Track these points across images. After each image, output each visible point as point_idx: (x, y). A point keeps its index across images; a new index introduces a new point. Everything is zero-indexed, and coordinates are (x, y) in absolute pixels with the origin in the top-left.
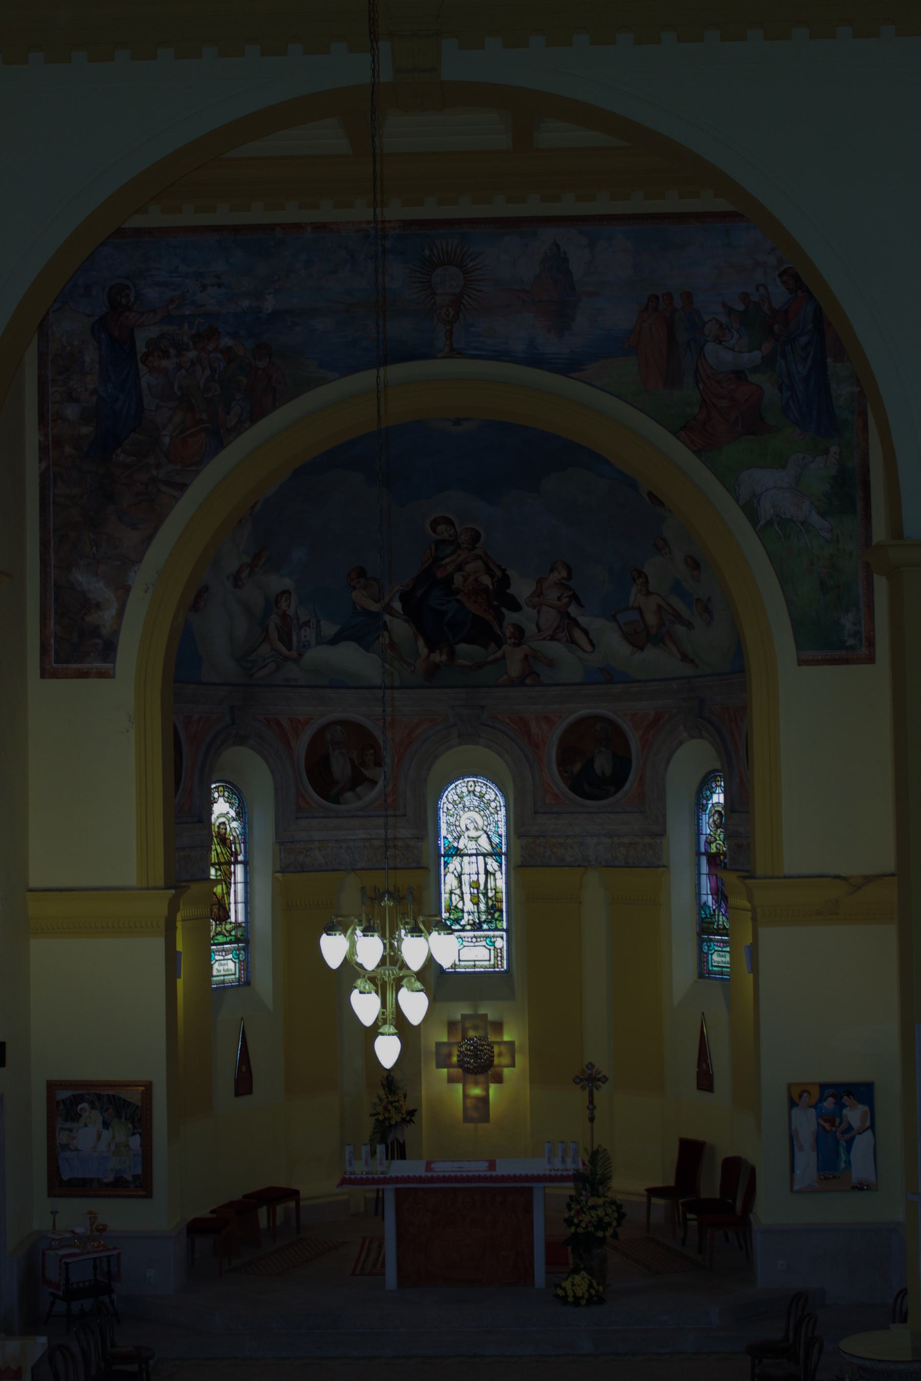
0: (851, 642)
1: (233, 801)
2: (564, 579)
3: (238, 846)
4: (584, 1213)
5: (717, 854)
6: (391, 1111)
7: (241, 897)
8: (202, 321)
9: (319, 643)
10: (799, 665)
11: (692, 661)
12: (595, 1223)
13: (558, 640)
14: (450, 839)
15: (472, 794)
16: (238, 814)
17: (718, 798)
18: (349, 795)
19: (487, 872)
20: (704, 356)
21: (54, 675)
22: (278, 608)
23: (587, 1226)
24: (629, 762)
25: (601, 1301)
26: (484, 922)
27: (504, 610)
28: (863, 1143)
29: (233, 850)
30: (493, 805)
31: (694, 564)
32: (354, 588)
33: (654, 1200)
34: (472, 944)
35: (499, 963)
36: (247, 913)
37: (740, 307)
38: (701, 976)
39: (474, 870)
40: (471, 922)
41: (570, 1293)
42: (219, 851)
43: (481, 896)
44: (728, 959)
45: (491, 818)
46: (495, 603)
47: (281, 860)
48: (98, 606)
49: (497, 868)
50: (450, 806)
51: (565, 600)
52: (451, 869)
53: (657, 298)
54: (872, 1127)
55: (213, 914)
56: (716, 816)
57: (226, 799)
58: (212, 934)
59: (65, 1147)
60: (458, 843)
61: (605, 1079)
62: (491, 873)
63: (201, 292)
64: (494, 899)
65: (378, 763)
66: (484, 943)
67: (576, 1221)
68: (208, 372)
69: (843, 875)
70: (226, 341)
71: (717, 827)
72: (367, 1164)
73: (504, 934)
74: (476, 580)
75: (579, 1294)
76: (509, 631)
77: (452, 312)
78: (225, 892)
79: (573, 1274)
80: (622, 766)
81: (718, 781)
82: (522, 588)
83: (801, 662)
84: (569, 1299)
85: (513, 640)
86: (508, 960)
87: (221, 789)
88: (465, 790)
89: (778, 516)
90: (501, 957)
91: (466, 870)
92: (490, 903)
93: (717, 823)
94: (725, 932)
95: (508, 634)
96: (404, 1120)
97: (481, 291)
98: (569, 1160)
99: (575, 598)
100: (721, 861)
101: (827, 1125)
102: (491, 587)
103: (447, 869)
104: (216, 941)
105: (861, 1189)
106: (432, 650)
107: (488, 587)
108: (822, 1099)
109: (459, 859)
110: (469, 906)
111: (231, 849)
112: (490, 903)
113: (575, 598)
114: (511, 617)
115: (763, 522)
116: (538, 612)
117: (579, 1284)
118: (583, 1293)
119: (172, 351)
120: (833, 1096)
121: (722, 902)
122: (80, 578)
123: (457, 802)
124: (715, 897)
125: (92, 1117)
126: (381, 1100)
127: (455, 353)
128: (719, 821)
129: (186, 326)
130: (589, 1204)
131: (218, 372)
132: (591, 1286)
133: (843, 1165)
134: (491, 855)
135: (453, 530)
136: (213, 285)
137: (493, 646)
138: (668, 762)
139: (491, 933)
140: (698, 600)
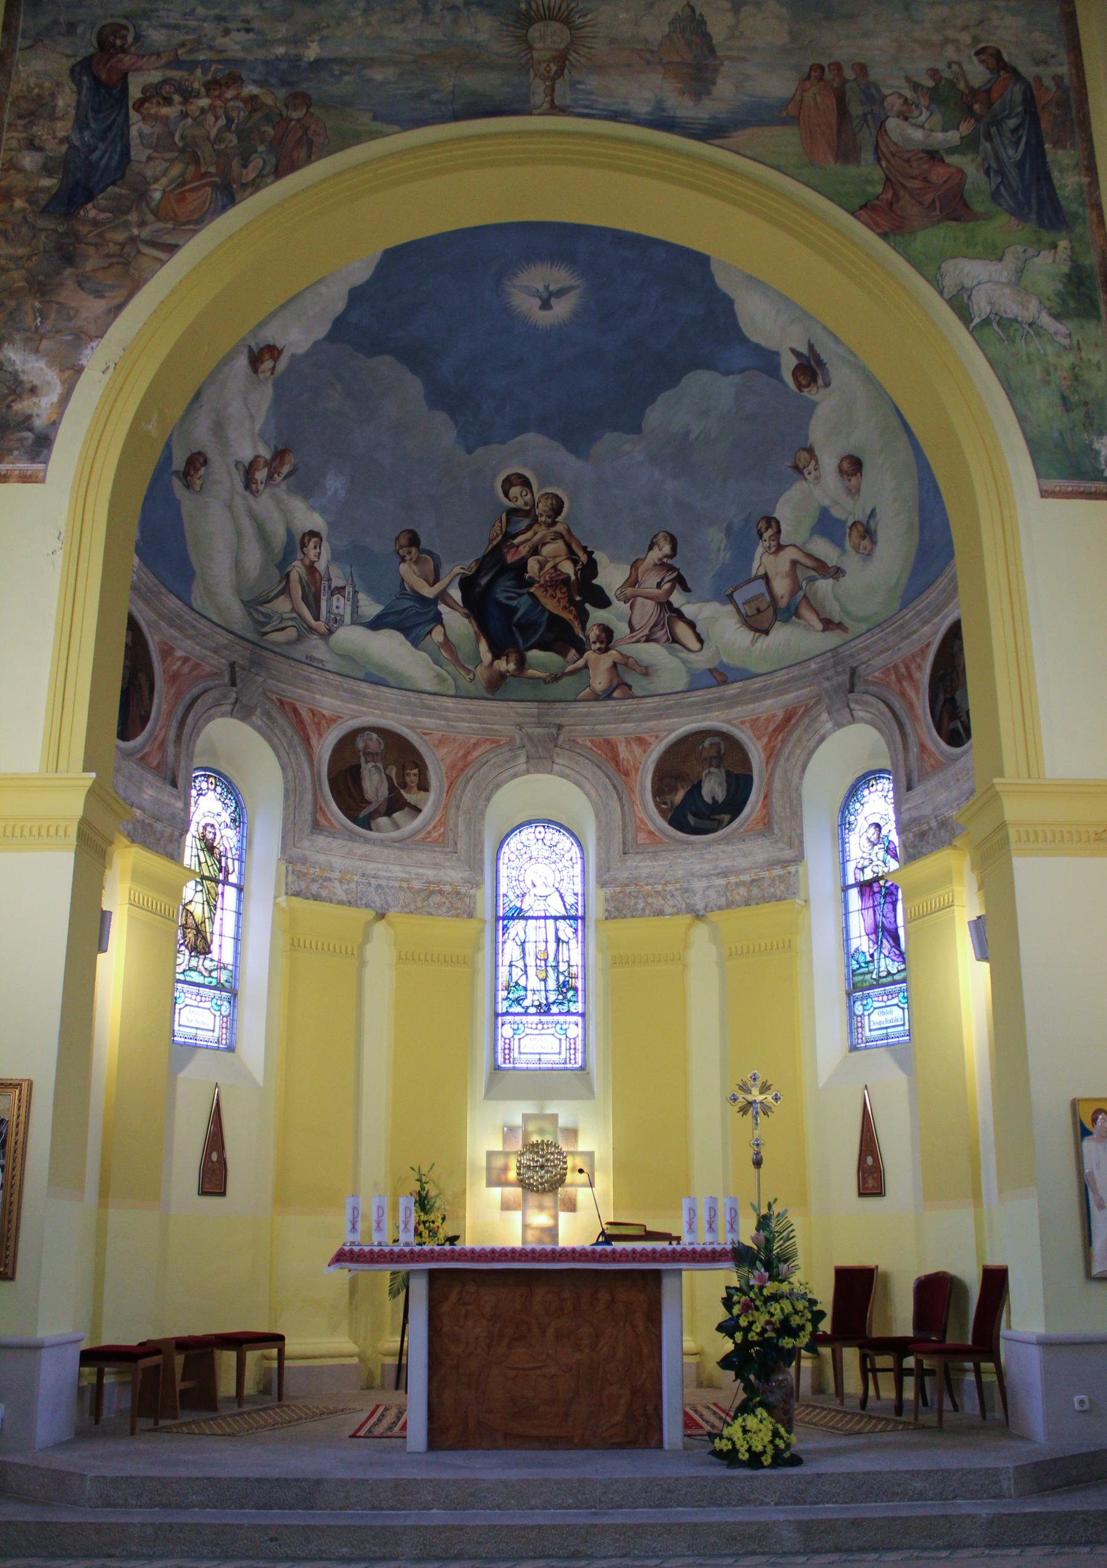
1: (226, 801)
2: (667, 556)
3: (230, 862)
4: (757, 1309)
5: (876, 879)
6: (423, 1234)
7: (229, 929)
8: (220, 67)
9: (354, 622)
10: (1042, 496)
11: (840, 625)
12: (778, 1325)
13: (656, 641)
14: (512, 897)
15: (540, 841)
16: (234, 820)
18: (383, 821)
19: (558, 940)
20: (886, 131)
22: (305, 554)
23: (764, 1330)
24: (748, 781)
25: (795, 1461)
26: (554, 1003)
27: (588, 606)
29: (223, 864)
30: (568, 856)
32: (403, 560)
34: (537, 1032)
35: (572, 1057)
36: (236, 954)
39: (542, 937)
40: (536, 1003)
41: (742, 1447)
42: (203, 859)
43: (549, 969)
45: (565, 873)
46: (578, 598)
47: (287, 884)
49: (571, 935)
50: (512, 857)
51: (667, 586)
52: (511, 937)
53: (822, 68)
55: (187, 939)
56: (872, 830)
57: (218, 797)
58: (180, 969)
60: (522, 901)
62: (563, 942)
63: (224, 36)
64: (566, 974)
65: (424, 787)
66: (552, 1031)
67: (743, 1322)
68: (222, 122)
70: (251, 89)
71: (874, 845)
73: (579, 1019)
74: (555, 567)
76: (593, 633)
77: (554, 68)
78: (207, 915)
79: (742, 1414)
81: (872, 786)
84: (740, 1456)
85: (598, 645)
86: (584, 1052)
87: (211, 780)
88: (532, 836)
89: (996, 314)
90: (575, 1049)
91: (531, 937)
92: (562, 978)
93: (872, 839)
94: (889, 979)
95: (592, 637)
97: (592, 48)
99: (680, 582)
100: (881, 887)
102: (573, 577)
103: (506, 935)
104: (188, 979)
106: (496, 656)
109: (522, 922)
110: (534, 983)
111: (220, 863)
112: (562, 978)
113: (680, 582)
114: (597, 615)
115: (976, 321)
116: (632, 607)
118: (765, 1447)
119: (177, 98)
121: (884, 941)
123: (522, 852)
124: (873, 937)
127: (555, 109)
128: (875, 836)
129: (199, 72)
130: (765, 1292)
131: (236, 121)
132: (776, 1434)
134: (564, 918)
135: (529, 496)
136: (239, 30)
138: (804, 768)
139: (562, 1019)
140: (854, 524)
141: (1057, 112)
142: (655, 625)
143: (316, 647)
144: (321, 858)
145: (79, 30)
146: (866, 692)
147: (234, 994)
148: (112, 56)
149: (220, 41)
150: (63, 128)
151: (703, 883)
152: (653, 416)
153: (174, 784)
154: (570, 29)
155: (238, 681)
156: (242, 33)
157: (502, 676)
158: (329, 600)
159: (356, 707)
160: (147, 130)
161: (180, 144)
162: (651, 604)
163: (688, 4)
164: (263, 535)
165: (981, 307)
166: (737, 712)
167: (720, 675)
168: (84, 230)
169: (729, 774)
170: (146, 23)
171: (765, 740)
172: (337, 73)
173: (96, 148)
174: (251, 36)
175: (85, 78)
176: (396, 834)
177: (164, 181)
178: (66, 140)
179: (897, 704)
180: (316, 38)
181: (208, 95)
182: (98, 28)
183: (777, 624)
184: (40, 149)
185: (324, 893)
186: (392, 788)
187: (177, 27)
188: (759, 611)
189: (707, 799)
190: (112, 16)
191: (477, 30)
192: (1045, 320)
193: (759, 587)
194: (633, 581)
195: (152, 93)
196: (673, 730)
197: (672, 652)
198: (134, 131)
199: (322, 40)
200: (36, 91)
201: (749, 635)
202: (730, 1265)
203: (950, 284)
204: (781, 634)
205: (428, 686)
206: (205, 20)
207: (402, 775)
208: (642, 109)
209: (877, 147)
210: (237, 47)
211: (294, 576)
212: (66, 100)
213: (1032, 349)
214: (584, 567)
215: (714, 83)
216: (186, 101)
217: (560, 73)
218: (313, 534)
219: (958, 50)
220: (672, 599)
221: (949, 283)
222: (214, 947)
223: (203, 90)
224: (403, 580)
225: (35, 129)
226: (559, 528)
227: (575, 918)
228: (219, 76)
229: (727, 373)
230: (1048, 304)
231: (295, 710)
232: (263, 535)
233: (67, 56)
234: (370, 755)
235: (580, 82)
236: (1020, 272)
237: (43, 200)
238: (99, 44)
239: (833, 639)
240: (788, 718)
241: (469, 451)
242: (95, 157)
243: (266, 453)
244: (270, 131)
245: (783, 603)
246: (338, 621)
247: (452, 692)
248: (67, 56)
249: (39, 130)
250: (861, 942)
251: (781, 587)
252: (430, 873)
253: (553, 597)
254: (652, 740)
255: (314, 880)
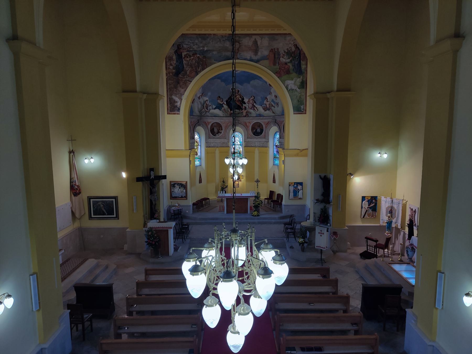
0: (302, 110)
5: (277, 145)
17: (278, 136)
18: (217, 135)
19: (239, 148)
21: (170, 114)
25: (259, 216)
28: (301, 192)
31: (276, 97)
32: (218, 100)
33: (266, 200)
37: (287, 51)
38: (274, 165)
44: (279, 162)
48: (177, 102)
53: (272, 49)
54: (302, 189)
59: (173, 192)
61: (255, 181)
65: (222, 130)
69: (300, 149)
70: (198, 55)
72: (222, 194)
75: (256, 215)
76: (244, 108)
80: (262, 131)
82: (246, 100)
83: (294, 114)
96: (226, 187)
98: (254, 194)
99: (255, 102)
101: (295, 189)
105: (300, 199)
106: (231, 111)
107: (240, 100)
108: (294, 185)
113: (255, 102)
114: (244, 105)
117: (256, 213)
119: (189, 57)
120: (296, 184)
122: (173, 97)
125: (177, 187)
126: (222, 184)
129: (191, 52)
132: (257, 213)
133: (297, 195)
136: (196, 45)
137: (241, 110)
141: (303, 55)
142: (252, 107)
143: (208, 114)
144: (210, 141)
145: (175, 45)
146: (277, 123)
147: (201, 159)
148: (180, 50)
149: (194, 47)
150: (175, 62)
151: (257, 143)
152: (252, 82)
153: (193, 139)
154: (240, 44)
155: (199, 122)
156: (196, 45)
157: (232, 113)
158: (209, 107)
159: (213, 120)
160: (186, 62)
161: (190, 65)
162: (251, 104)
163: (255, 39)
164: (201, 103)
165: (289, 88)
166: (262, 120)
167: (260, 115)
168: (180, 78)
169: (261, 129)
170: (183, 44)
171: (265, 125)
172: (209, 52)
173: (179, 65)
174: (197, 46)
175: (176, 54)
176: (219, 136)
177: (189, 71)
178: (175, 64)
179: (280, 126)
180: (206, 46)
181: (193, 57)
182: (177, 45)
183: (267, 110)
184: (172, 65)
185: (210, 145)
186: (218, 130)
187: (187, 44)
188: (265, 108)
189: (258, 131)
190: (179, 43)
191: (227, 45)
192: (298, 89)
193: (265, 105)
194: (249, 101)
195: (185, 56)
196: (254, 121)
197: (254, 111)
198: (184, 63)
199: (207, 46)
200: (170, 56)
201: (263, 111)
202: (254, 198)
203: (286, 84)
204: (267, 112)
205: (222, 116)
206: (191, 43)
207: (219, 128)
208: (249, 58)
209: (279, 63)
210: (196, 48)
211: (205, 106)
212: (174, 57)
213: (295, 93)
214: (242, 99)
215: (258, 53)
216: (190, 58)
217: (238, 52)
218: (207, 100)
219: (291, 45)
220: (254, 104)
221: (286, 84)
222: (198, 154)
223: (192, 56)
224: (218, 102)
225: (171, 62)
226: (239, 94)
227: (241, 145)
228: (194, 53)
229: (261, 81)
230: (298, 86)
231: (206, 123)
232: (201, 103)
233: (173, 50)
234: (215, 126)
235: (240, 54)
236: (295, 82)
237: (174, 74)
238: (177, 47)
239: (273, 115)
240: (268, 123)
241: (227, 86)
242: (180, 66)
243: (201, 94)
244: (201, 62)
245: (268, 108)
246: (210, 110)
247: (225, 116)
248: (173, 50)
249: (172, 62)
250: (276, 153)
251: (268, 106)
252: (223, 141)
253: (238, 102)
254: (251, 122)
255: (209, 144)
